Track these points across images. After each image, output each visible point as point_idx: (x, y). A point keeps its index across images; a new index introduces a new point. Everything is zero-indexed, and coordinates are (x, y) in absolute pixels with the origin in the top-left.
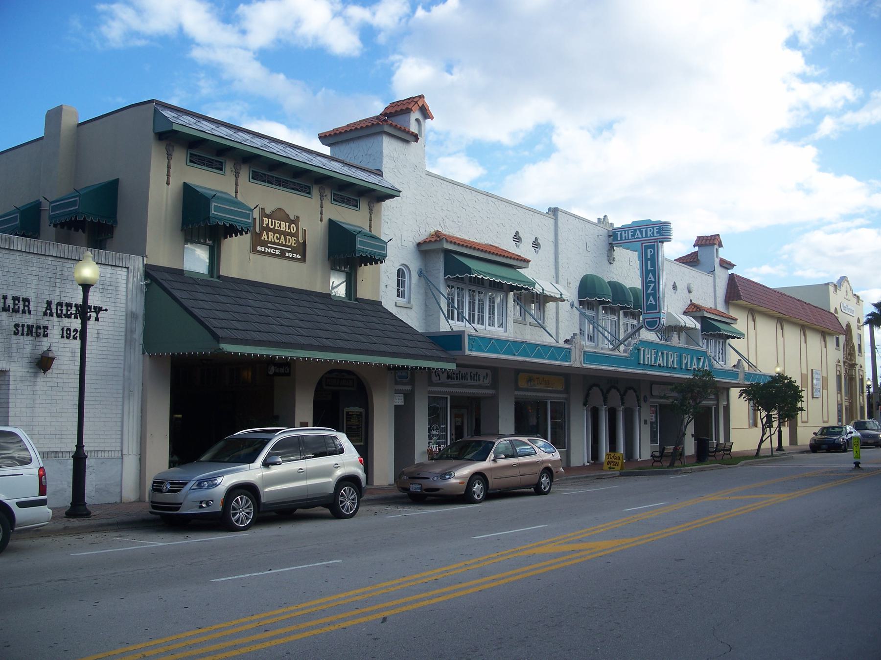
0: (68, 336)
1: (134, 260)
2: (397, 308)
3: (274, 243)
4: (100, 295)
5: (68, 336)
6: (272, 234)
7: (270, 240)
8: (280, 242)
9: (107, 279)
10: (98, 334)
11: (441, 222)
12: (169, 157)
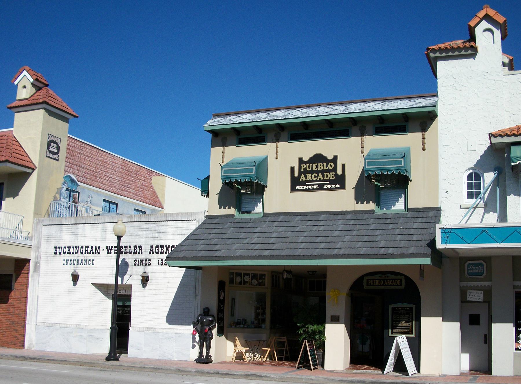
0: (162, 264)
5: (162, 264)
6: (310, 175)
7: (308, 179)
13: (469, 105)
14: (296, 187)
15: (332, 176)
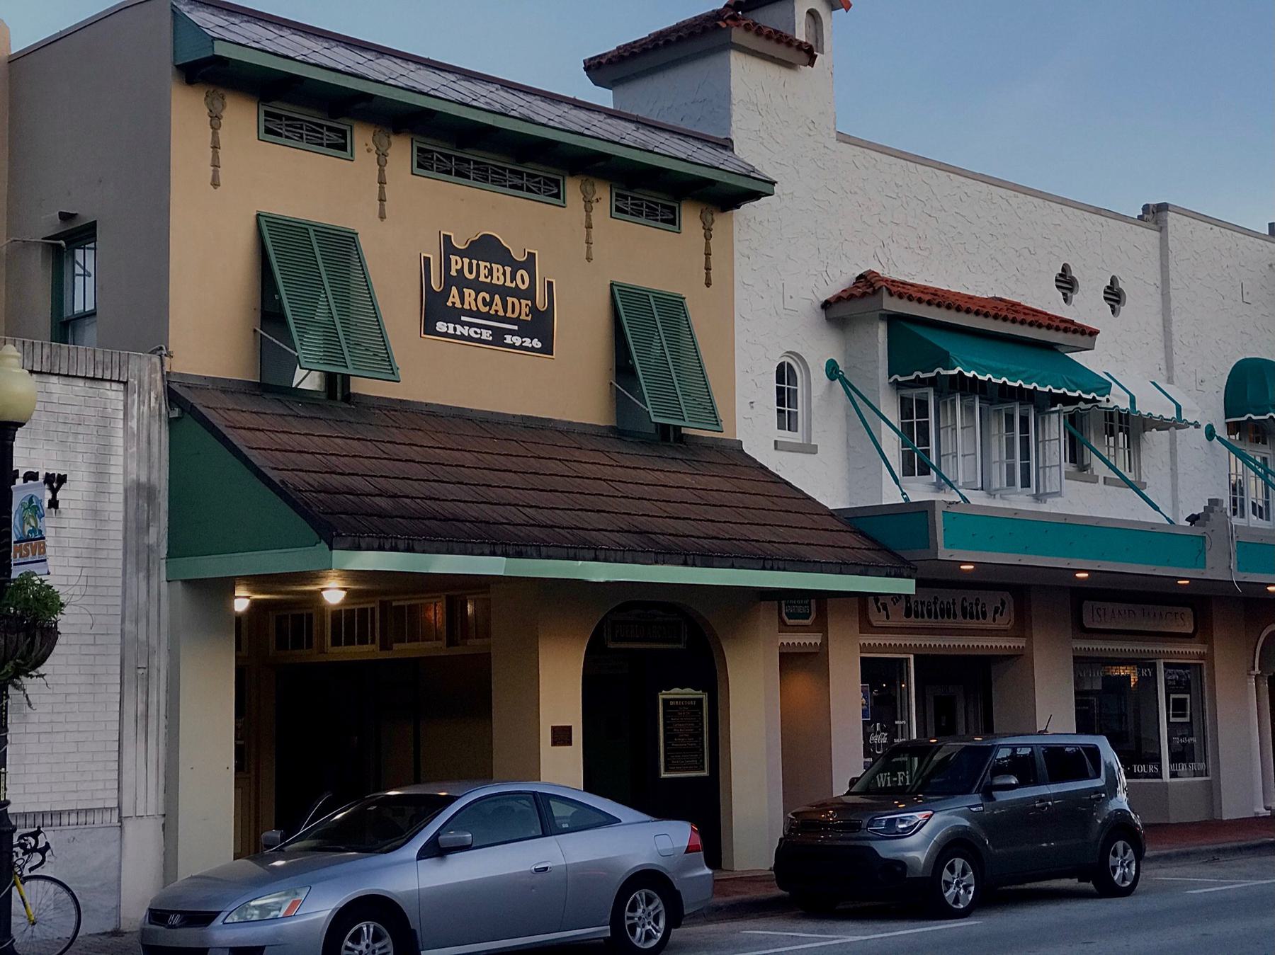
3: (478, 314)
8: (492, 312)
11: (878, 250)
13: (783, 194)
15: (525, 310)
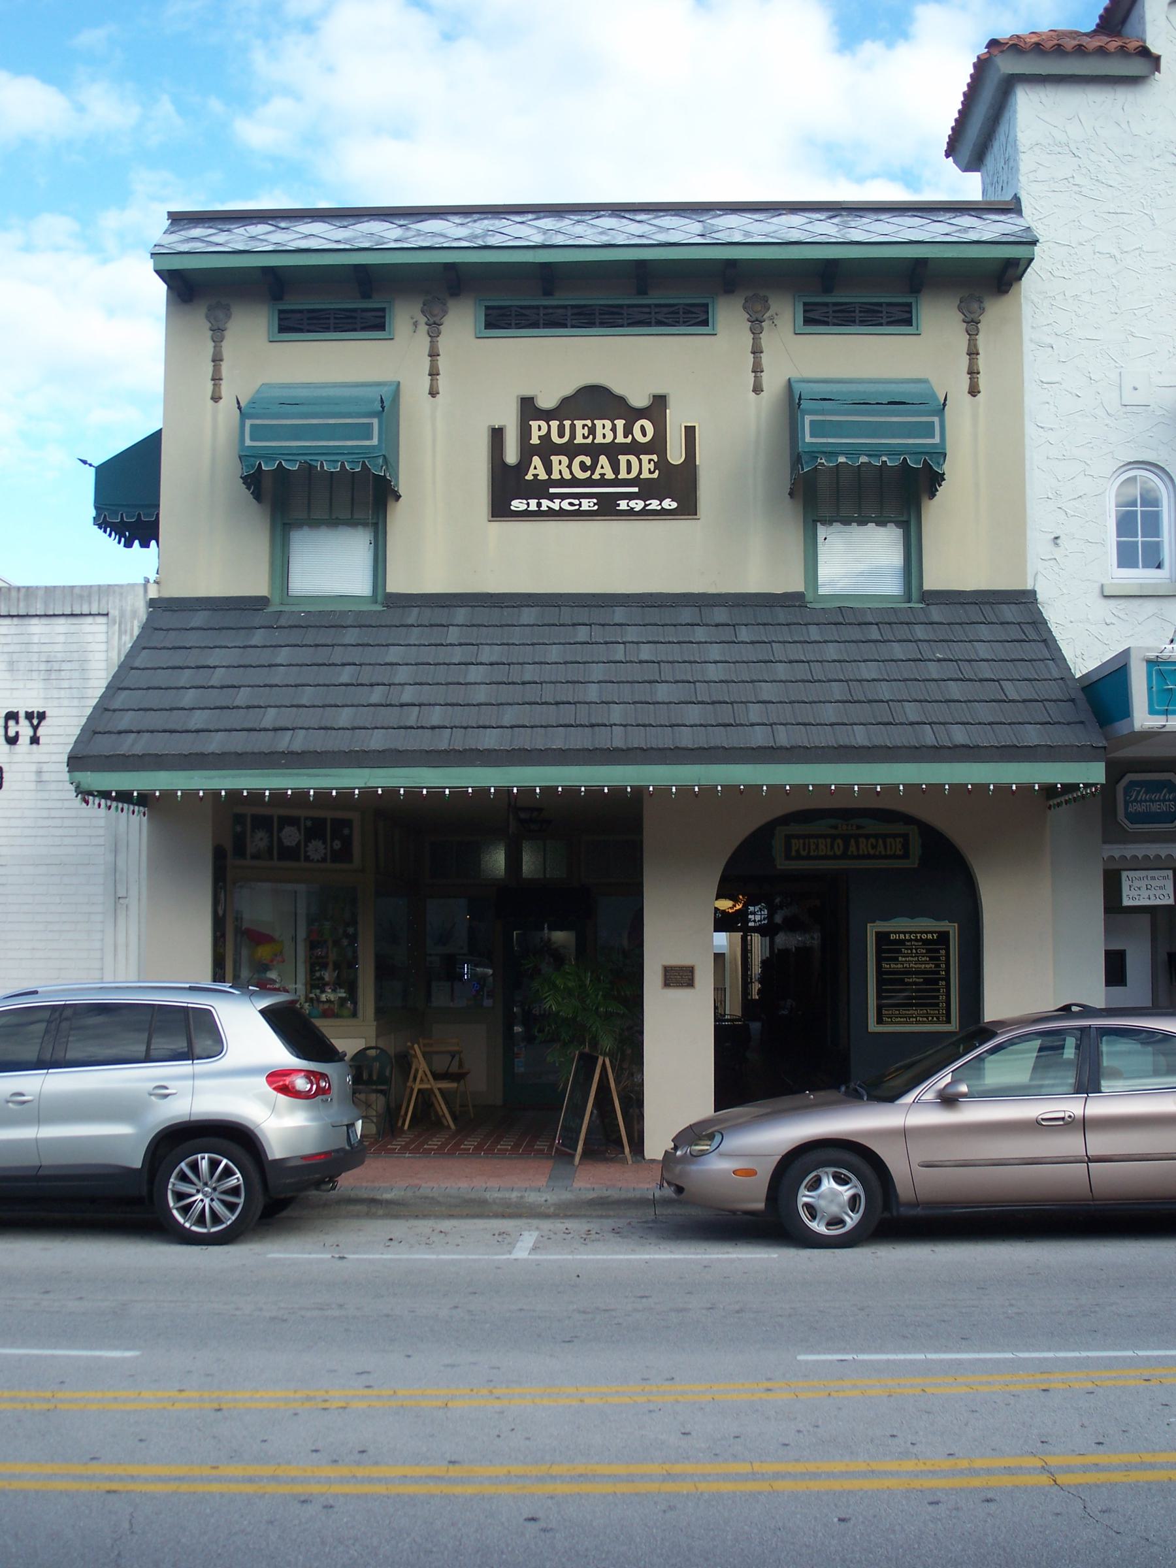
1: (121, 594)
2: (1112, 603)
3: (574, 482)
4: (41, 685)
7: (555, 476)
9: (58, 648)
10: (39, 772)
12: (218, 334)
14: (513, 503)
15: (646, 466)
